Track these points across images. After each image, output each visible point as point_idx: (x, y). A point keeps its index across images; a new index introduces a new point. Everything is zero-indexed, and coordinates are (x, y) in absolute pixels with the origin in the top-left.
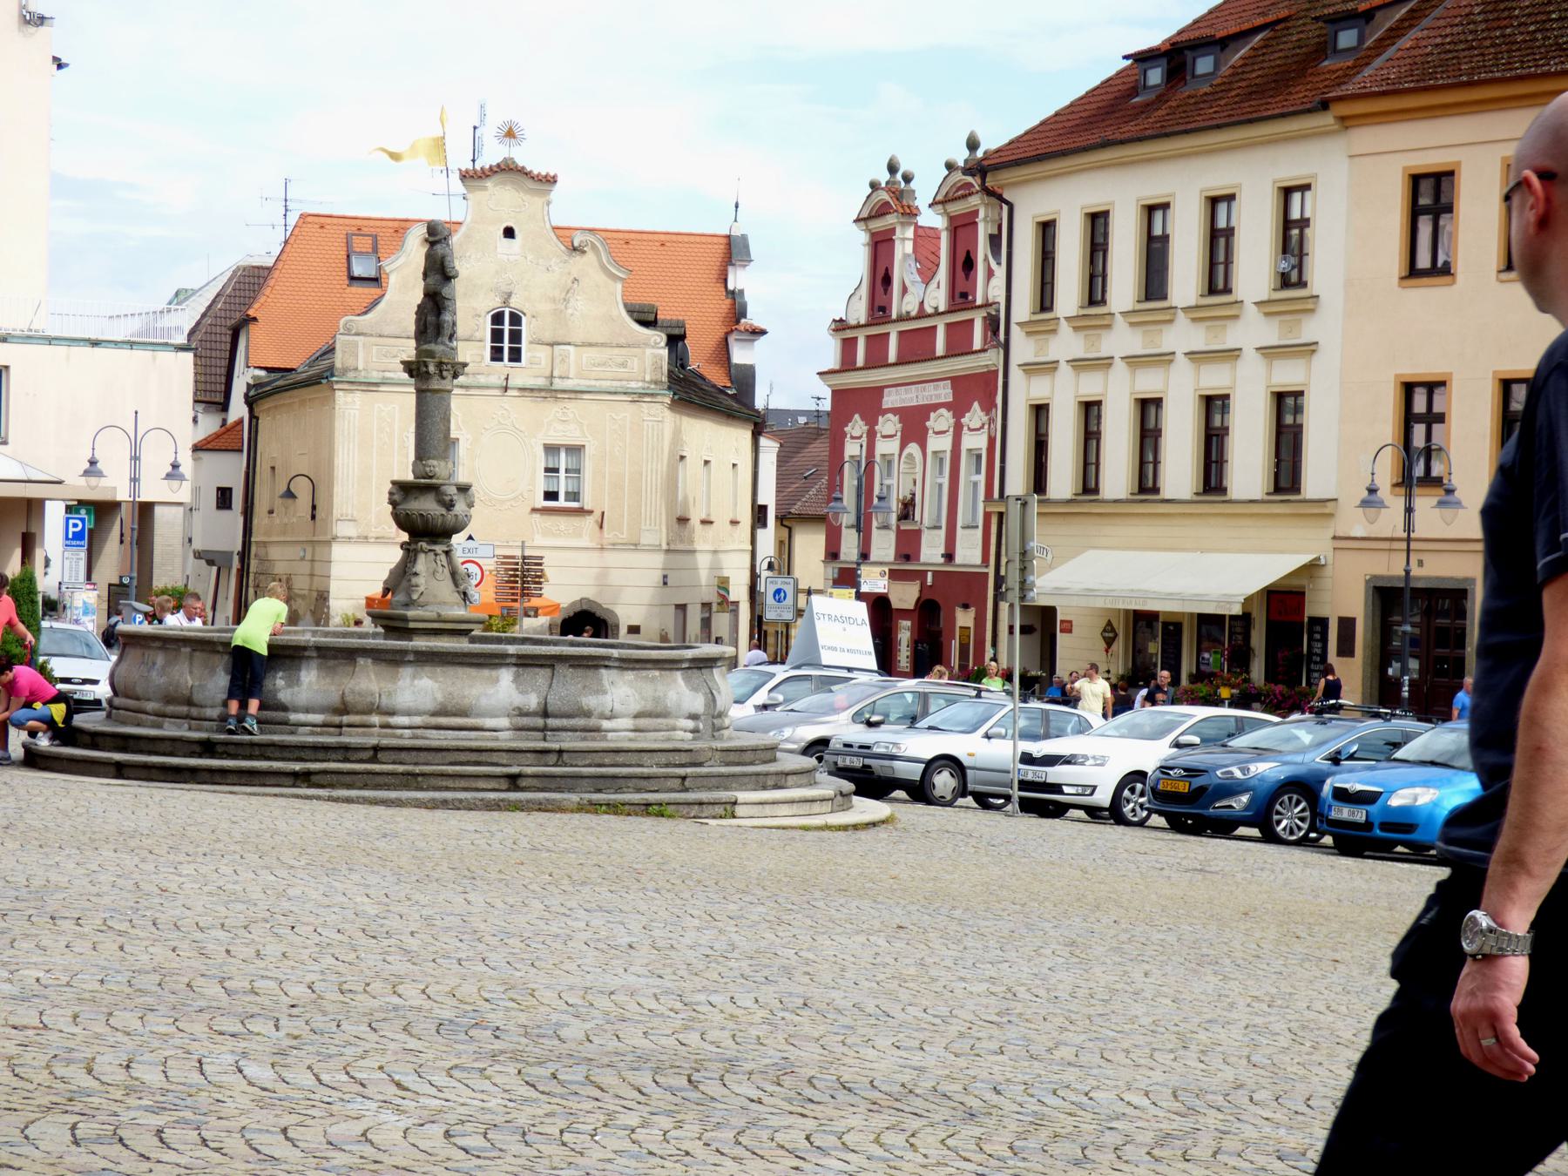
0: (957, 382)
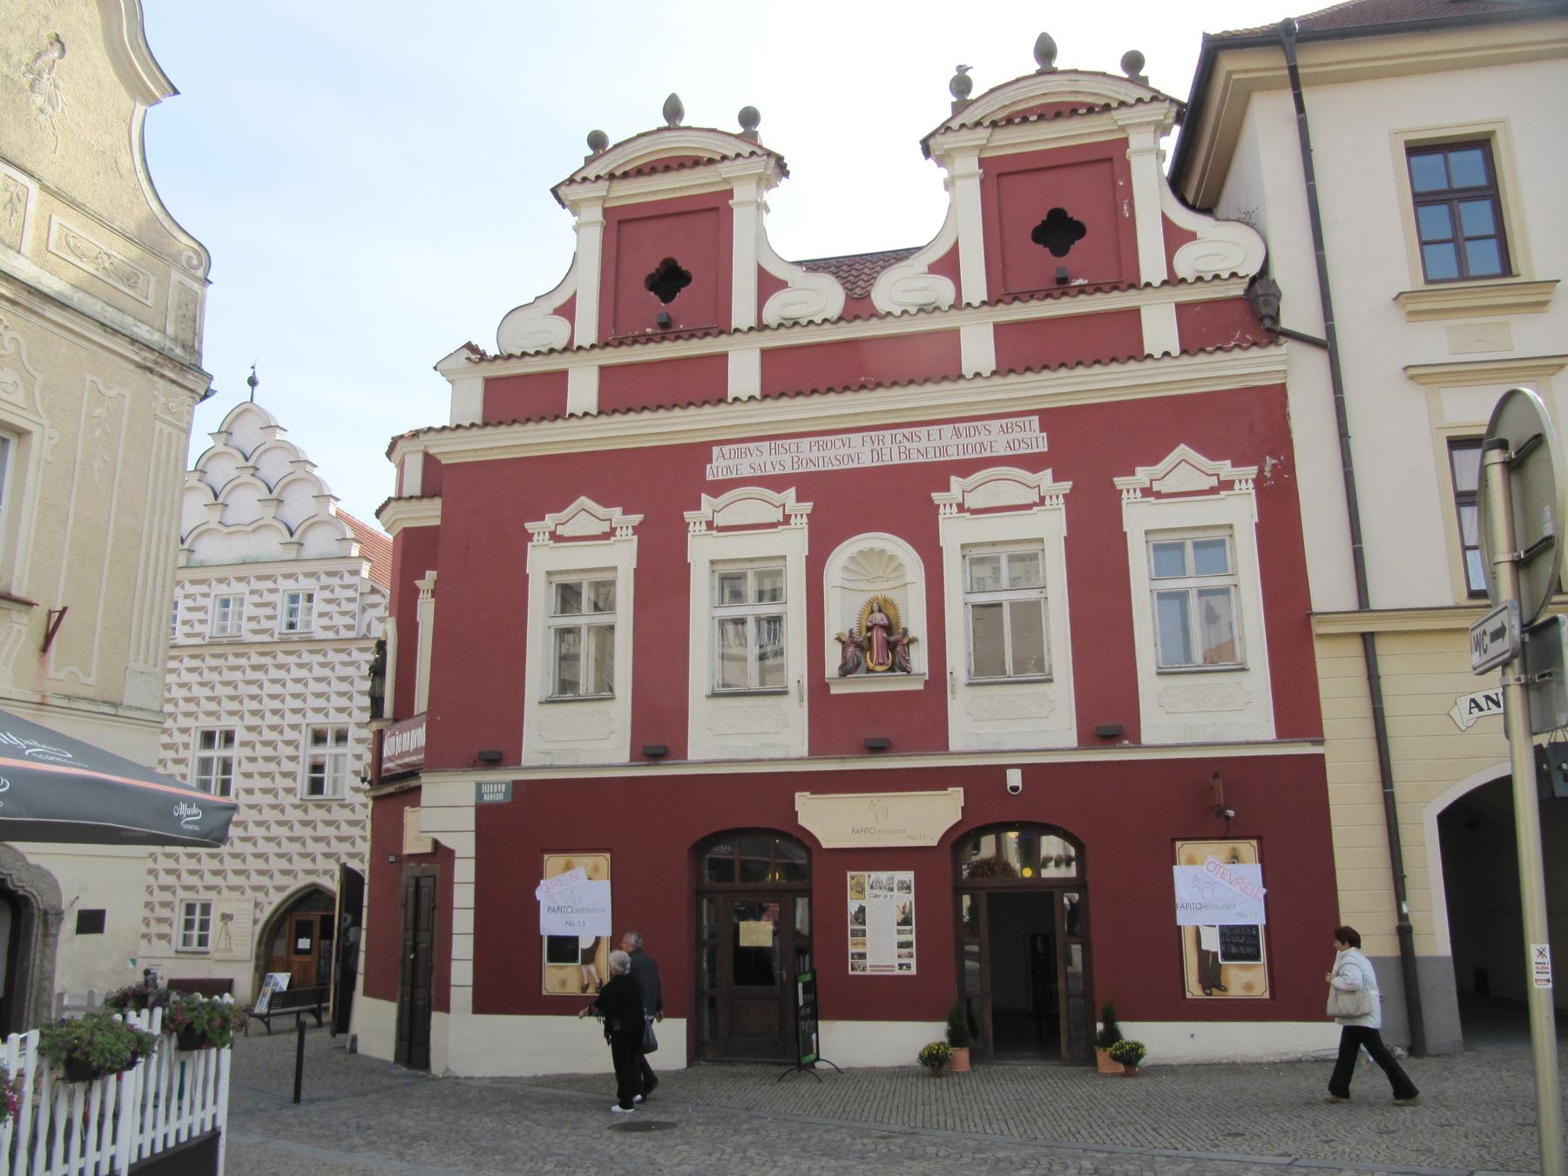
0: (1051, 419)
